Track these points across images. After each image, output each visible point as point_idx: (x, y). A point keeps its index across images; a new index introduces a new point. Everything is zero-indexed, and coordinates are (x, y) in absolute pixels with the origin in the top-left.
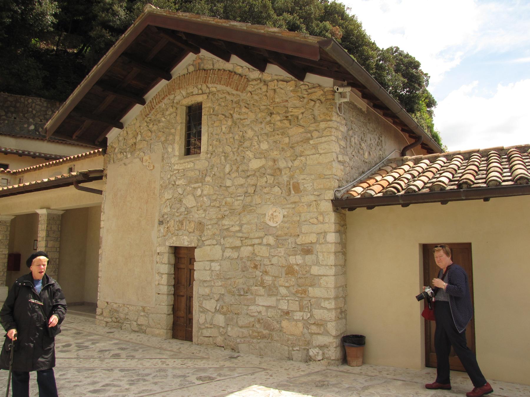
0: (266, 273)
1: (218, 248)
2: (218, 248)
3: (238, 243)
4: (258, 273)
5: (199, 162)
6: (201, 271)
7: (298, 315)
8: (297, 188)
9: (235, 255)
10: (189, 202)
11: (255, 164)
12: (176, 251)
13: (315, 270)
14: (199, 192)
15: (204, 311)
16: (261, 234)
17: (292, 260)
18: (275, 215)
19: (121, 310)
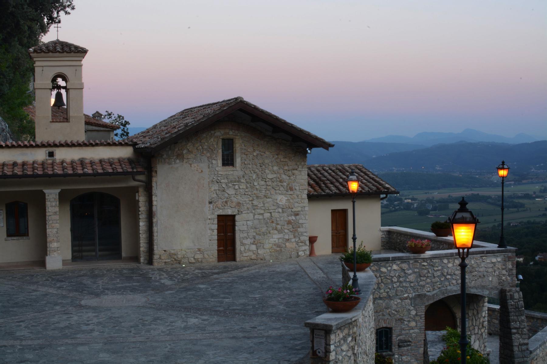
3: (262, 212)
7: (293, 240)
8: (291, 189)
9: (261, 217)
10: (231, 192)
13: (301, 221)
14: (237, 187)
15: (243, 244)
17: (290, 218)
18: (282, 199)
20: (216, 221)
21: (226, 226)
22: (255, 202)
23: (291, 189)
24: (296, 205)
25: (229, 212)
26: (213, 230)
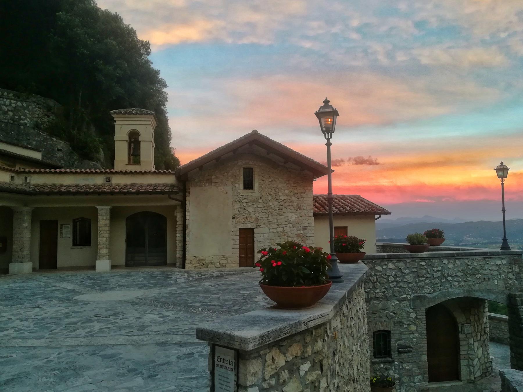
0: (289, 237)
1: (267, 228)
2: (267, 228)
3: (276, 226)
4: (286, 237)
5: (255, 193)
6: (257, 237)
8: (300, 209)
9: (275, 230)
10: (251, 209)
11: (283, 198)
12: (241, 229)
13: (308, 235)
14: (255, 206)
16: (286, 223)
17: (299, 232)
18: (292, 217)
19: (207, 259)
20: (238, 233)
21: (247, 236)
22: (270, 219)
23: (300, 209)
24: (304, 221)
25: (249, 226)
26: (235, 240)
